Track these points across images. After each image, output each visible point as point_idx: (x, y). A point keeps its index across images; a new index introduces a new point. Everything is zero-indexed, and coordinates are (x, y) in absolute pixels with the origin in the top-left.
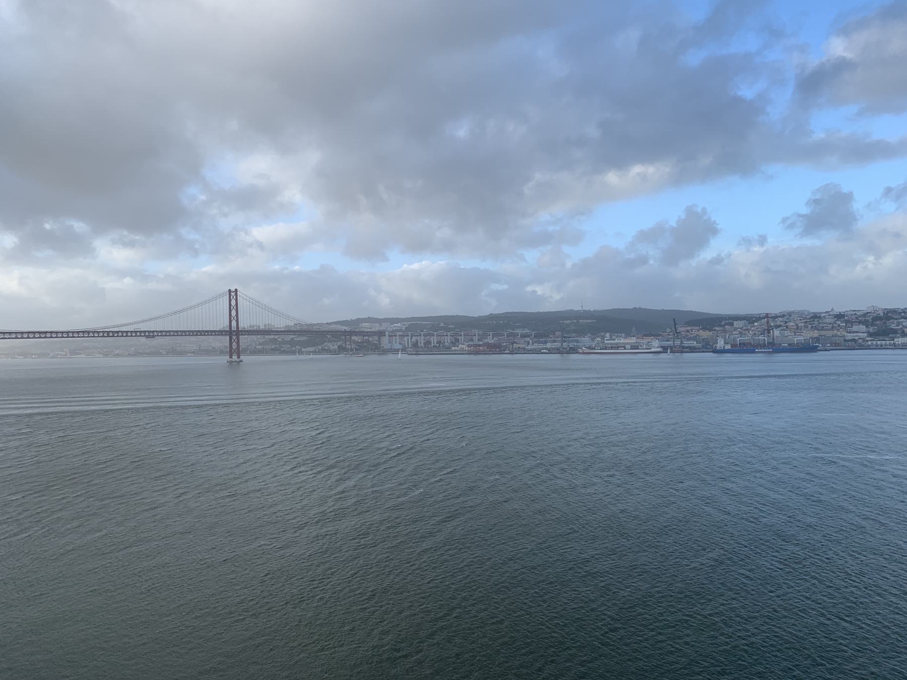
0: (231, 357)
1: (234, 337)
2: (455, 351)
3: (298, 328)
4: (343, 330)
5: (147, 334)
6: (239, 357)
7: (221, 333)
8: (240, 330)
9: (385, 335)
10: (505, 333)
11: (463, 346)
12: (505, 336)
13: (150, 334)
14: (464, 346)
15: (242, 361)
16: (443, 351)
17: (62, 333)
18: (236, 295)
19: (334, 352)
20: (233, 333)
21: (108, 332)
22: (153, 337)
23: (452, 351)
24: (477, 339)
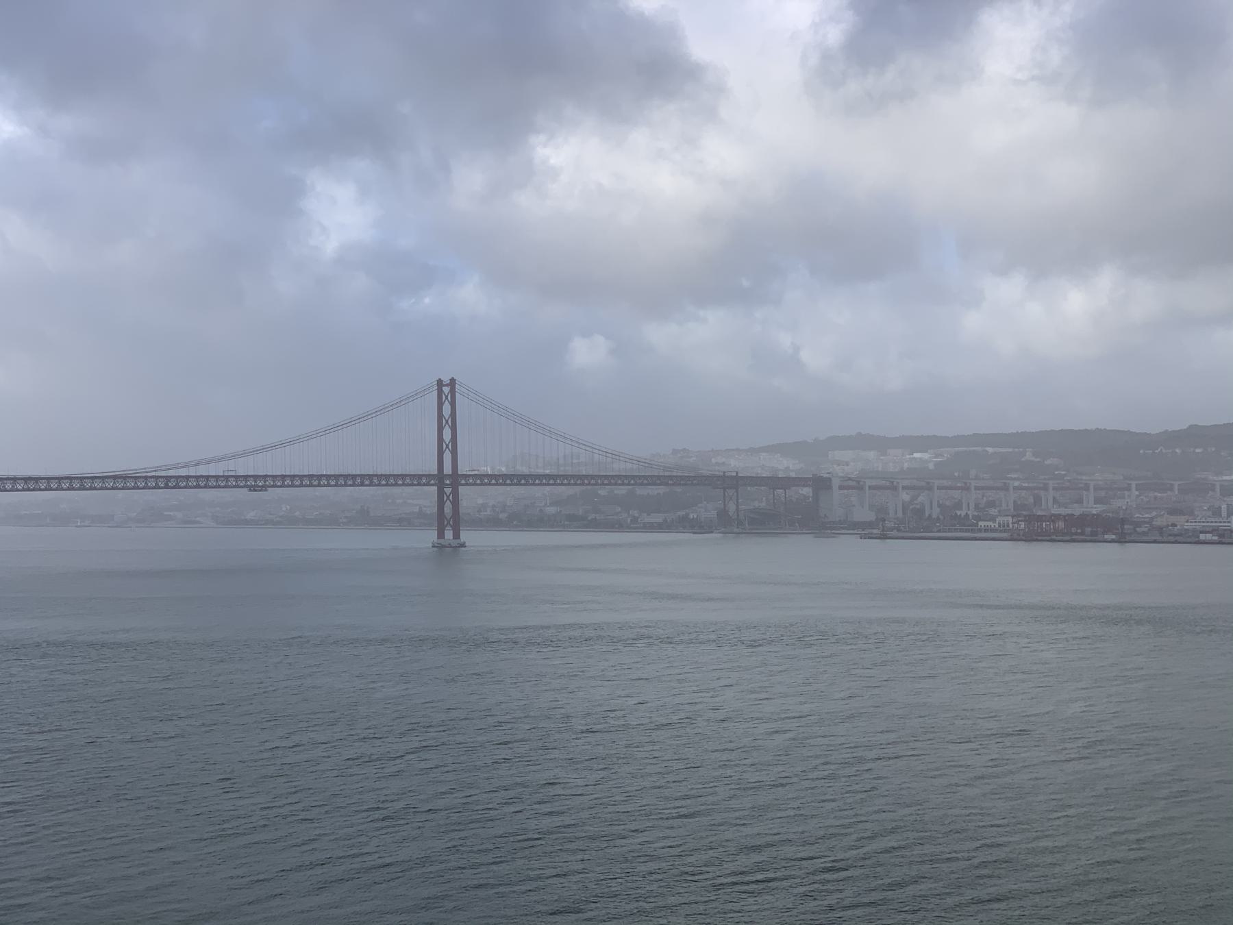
0: (441, 535)
1: (448, 490)
2: (986, 531)
4: (754, 475)
6: (457, 536)
7: (417, 480)
8: (459, 473)
9: (830, 487)
11: (1006, 519)
13: (257, 483)
15: (465, 547)
17: (70, 478)
18: (453, 392)
21: (168, 478)
22: (264, 488)
23: (980, 531)
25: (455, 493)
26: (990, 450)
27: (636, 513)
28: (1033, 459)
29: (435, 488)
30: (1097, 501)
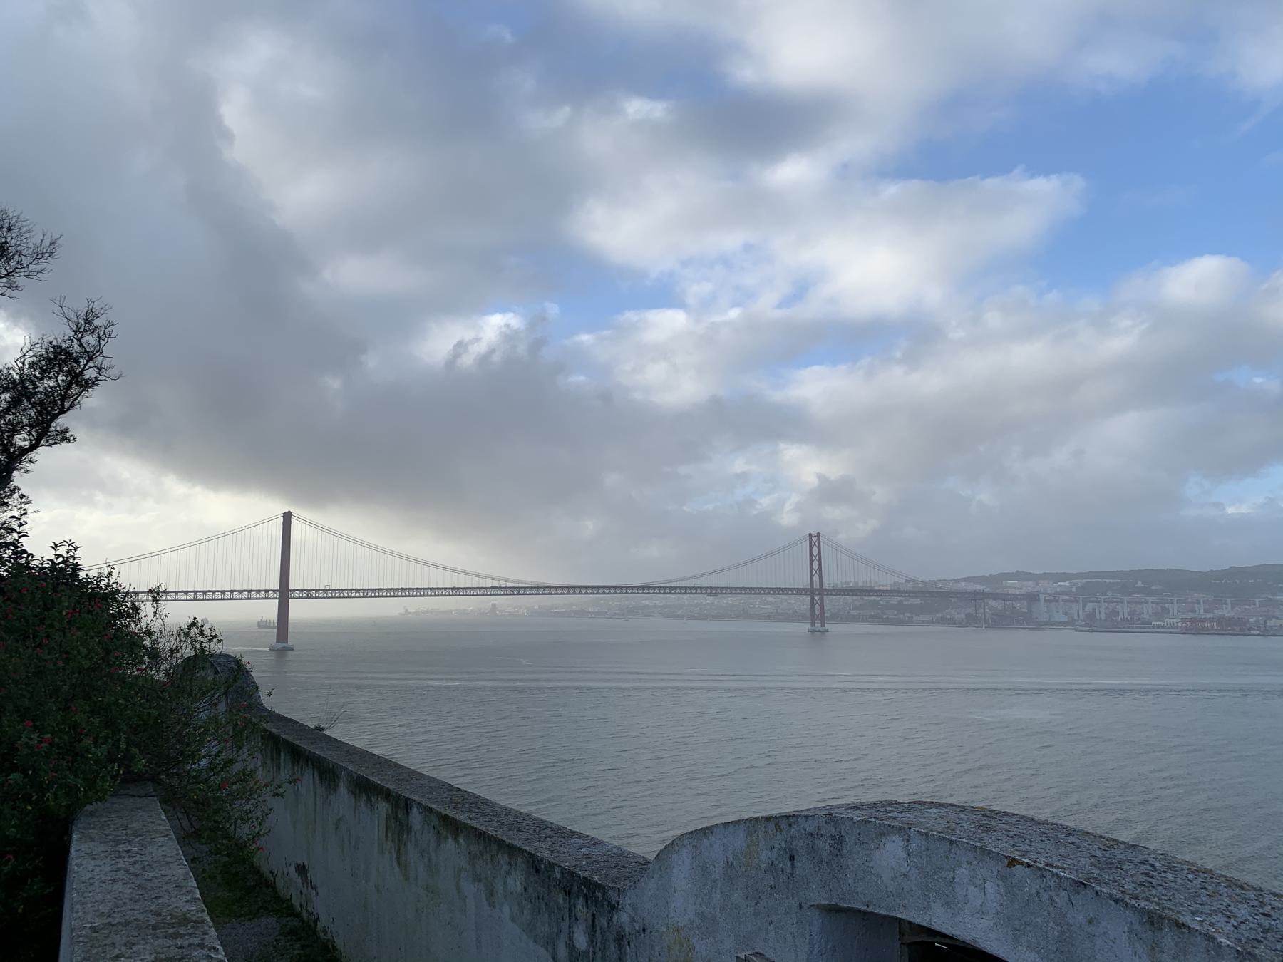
0: (813, 625)
2: (1158, 627)
3: (910, 586)
5: (709, 591)
6: (823, 625)
7: (799, 591)
9: (1039, 600)
10: (1257, 600)
11: (1172, 620)
12: (1258, 605)
13: (713, 592)
14: (1175, 620)
16: (1141, 627)
18: (819, 540)
19: (960, 624)
20: (817, 592)
21: (665, 588)
22: (716, 595)
23: (1153, 627)
24: (1202, 610)
25: (822, 599)
26: (1107, 581)
27: (909, 615)
28: (1143, 586)
29: (809, 598)
30: (1206, 611)
